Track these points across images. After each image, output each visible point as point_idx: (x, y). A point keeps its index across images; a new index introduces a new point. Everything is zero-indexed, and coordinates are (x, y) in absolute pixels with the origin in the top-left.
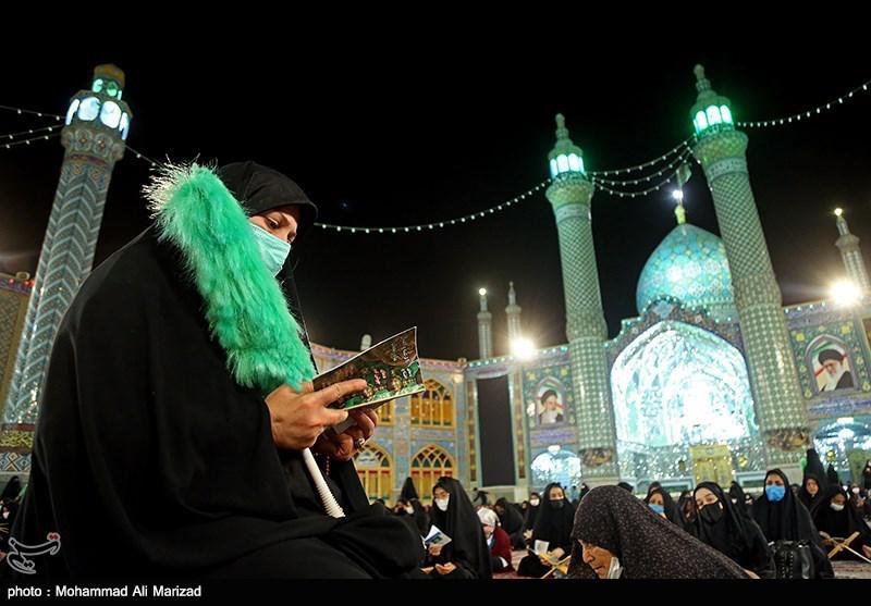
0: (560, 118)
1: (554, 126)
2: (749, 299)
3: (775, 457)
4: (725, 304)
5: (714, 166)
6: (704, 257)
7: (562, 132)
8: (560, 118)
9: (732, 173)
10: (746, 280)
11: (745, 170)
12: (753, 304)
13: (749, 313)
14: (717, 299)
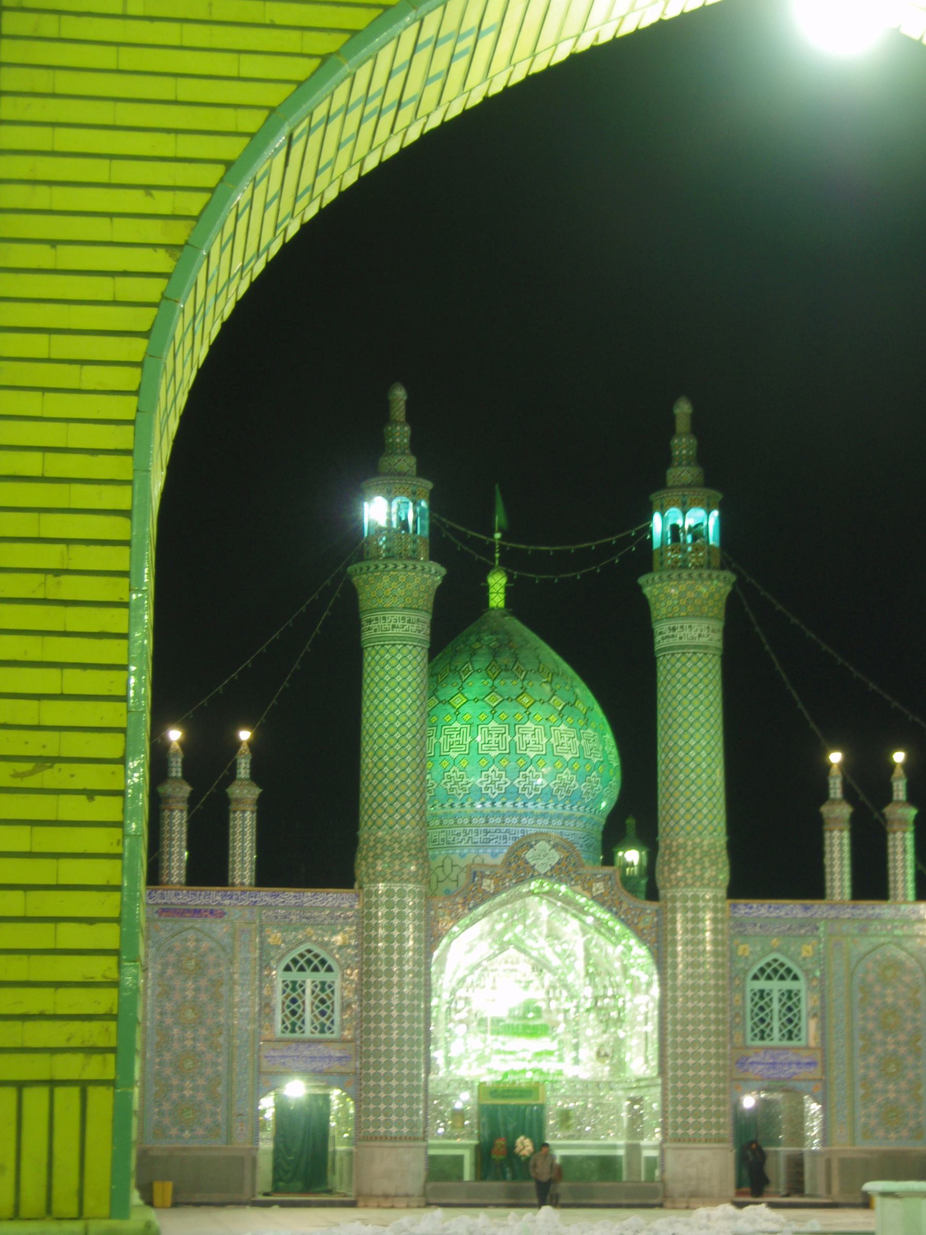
0: (400, 394)
1: (383, 416)
2: (689, 876)
3: (680, 1131)
4: (569, 817)
5: (677, 623)
6: (553, 718)
7: (400, 434)
8: (400, 394)
9: (707, 647)
10: (690, 843)
11: (720, 645)
12: (693, 885)
13: (685, 899)
14: (560, 806)
